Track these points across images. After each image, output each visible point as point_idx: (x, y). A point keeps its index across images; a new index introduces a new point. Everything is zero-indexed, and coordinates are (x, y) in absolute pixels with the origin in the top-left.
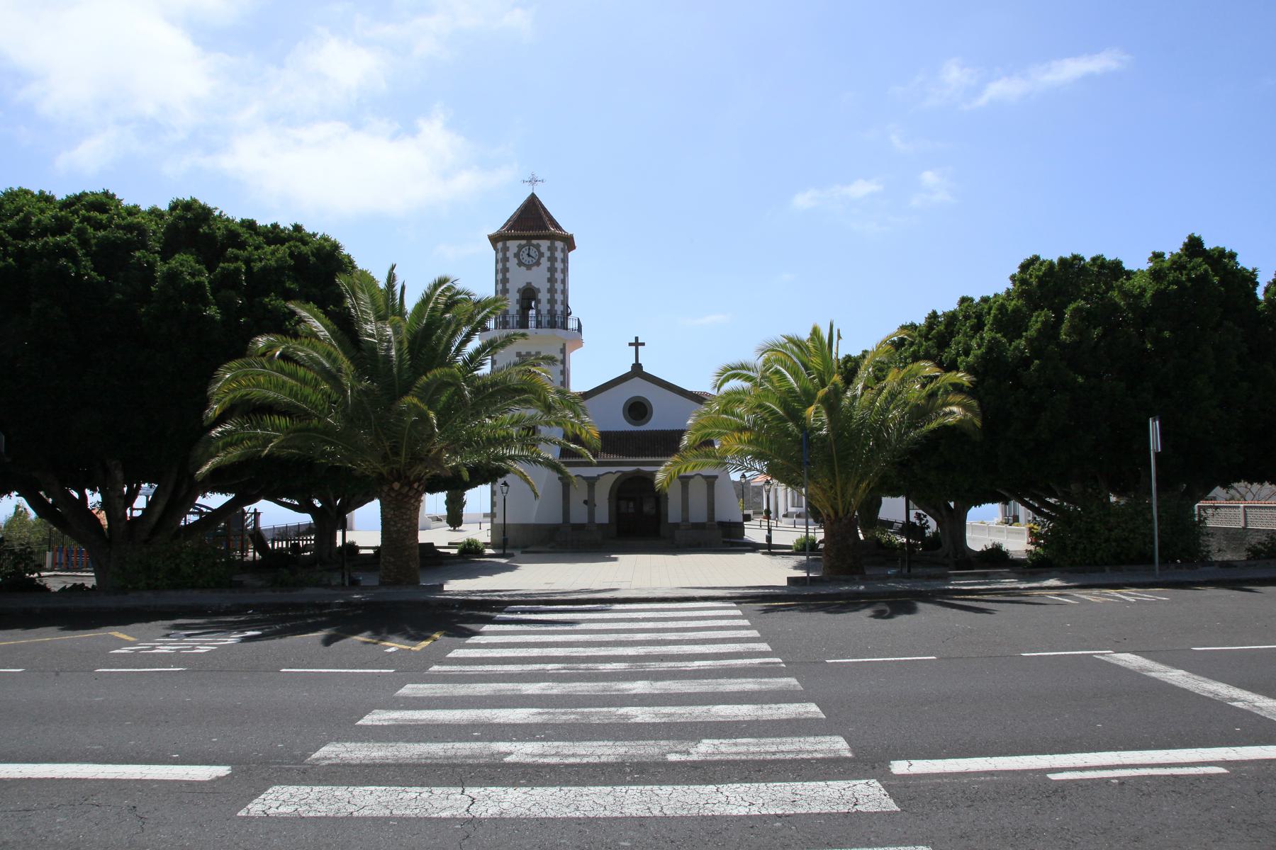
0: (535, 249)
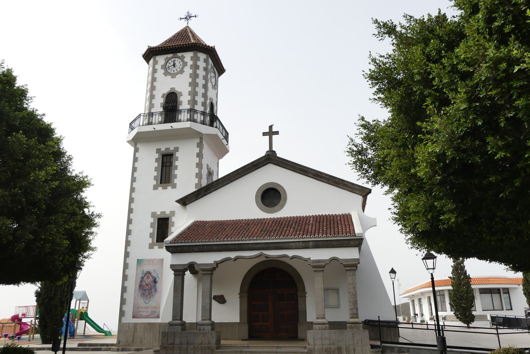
0: (180, 60)
